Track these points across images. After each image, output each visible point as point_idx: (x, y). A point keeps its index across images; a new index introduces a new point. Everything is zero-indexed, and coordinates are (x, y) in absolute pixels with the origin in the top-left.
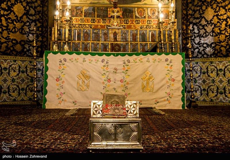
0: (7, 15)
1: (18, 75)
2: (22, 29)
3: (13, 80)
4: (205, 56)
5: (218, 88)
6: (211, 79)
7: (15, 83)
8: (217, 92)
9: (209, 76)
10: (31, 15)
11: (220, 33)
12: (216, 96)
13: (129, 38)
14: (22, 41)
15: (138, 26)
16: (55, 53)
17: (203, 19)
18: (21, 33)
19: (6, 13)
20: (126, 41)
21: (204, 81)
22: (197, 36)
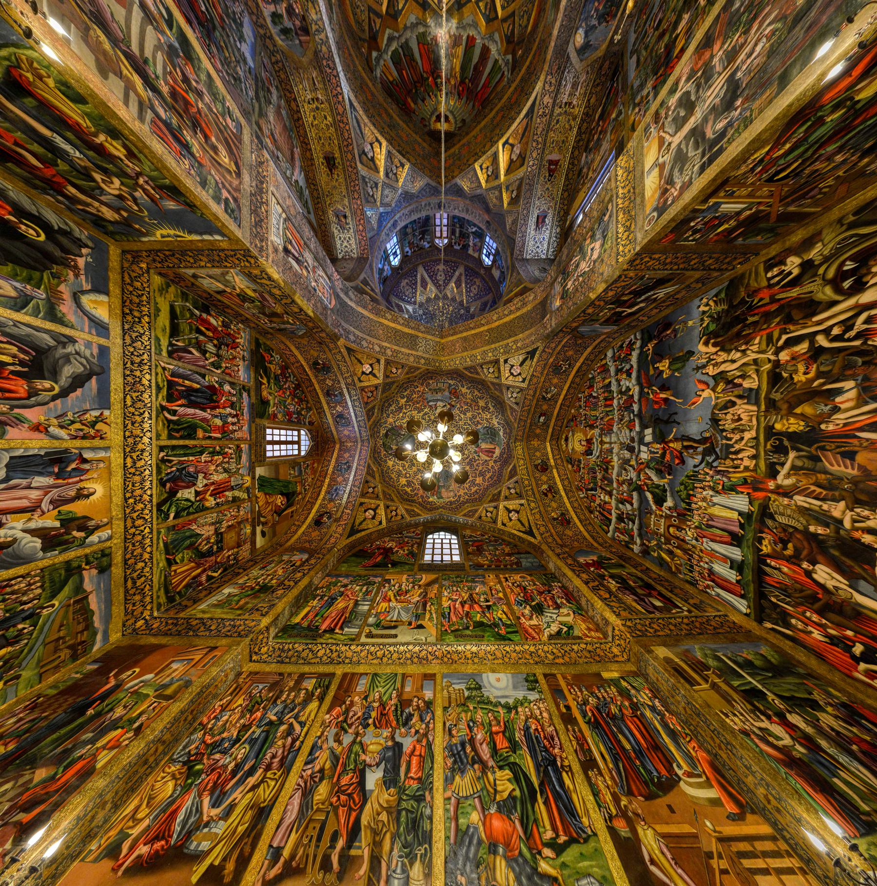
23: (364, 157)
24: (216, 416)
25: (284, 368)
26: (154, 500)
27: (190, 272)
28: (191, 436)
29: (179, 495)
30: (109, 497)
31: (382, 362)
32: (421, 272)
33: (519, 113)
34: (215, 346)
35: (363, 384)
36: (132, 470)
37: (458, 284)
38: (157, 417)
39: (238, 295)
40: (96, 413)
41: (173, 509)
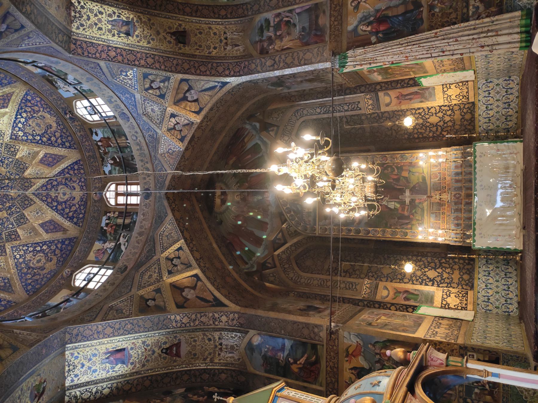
0: (437, 282)
1: (492, 277)
2: (449, 273)
3: (497, 281)
4: (473, 119)
5: (505, 108)
6: (495, 114)
7: (500, 280)
8: (508, 108)
9: (492, 116)
10: (436, 266)
11: (452, 110)
12: (512, 109)
13: (459, 185)
14: (460, 274)
15: (448, 178)
16: (474, 241)
17: (438, 124)
18: (452, 274)
19: (436, 283)
20: (461, 187)
21: (498, 119)
22: (454, 127)
32: (71, 156)
33: (218, 289)
37: (51, 226)
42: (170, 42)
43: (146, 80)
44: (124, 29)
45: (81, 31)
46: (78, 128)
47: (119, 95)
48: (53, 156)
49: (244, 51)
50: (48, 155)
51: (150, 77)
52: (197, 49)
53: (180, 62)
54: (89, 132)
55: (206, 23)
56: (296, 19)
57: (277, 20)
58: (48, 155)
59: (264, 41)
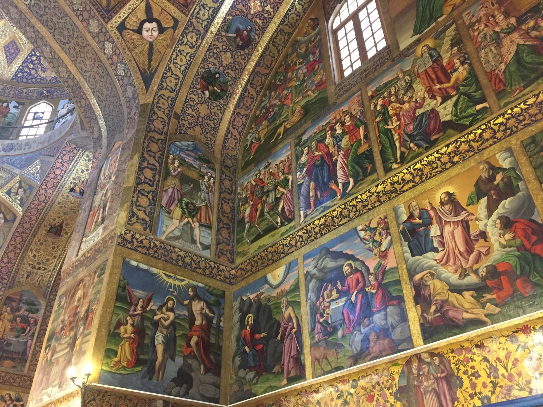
23: (8, 217)
24: (339, 147)
25: (257, 120)
26: (454, 139)
27: (207, 254)
28: (369, 155)
29: (448, 118)
30: (450, 181)
31: (117, 20)
34: (268, 196)
35: (178, 14)
36: (417, 179)
38: (354, 194)
39: (193, 217)
40: (362, 234)
41: (470, 111)
42: (54, 220)
43: (27, 187)
44: (77, 189)
45: (85, 157)
46: (31, 94)
47: (28, 156)
48: (14, 55)
49: (19, 282)
50: (17, 51)
51: (29, 191)
52: (39, 240)
53: (33, 222)
54: (21, 101)
55: (61, 254)
56: (20, 339)
57: (32, 321)
58: (17, 51)
59: (19, 304)
